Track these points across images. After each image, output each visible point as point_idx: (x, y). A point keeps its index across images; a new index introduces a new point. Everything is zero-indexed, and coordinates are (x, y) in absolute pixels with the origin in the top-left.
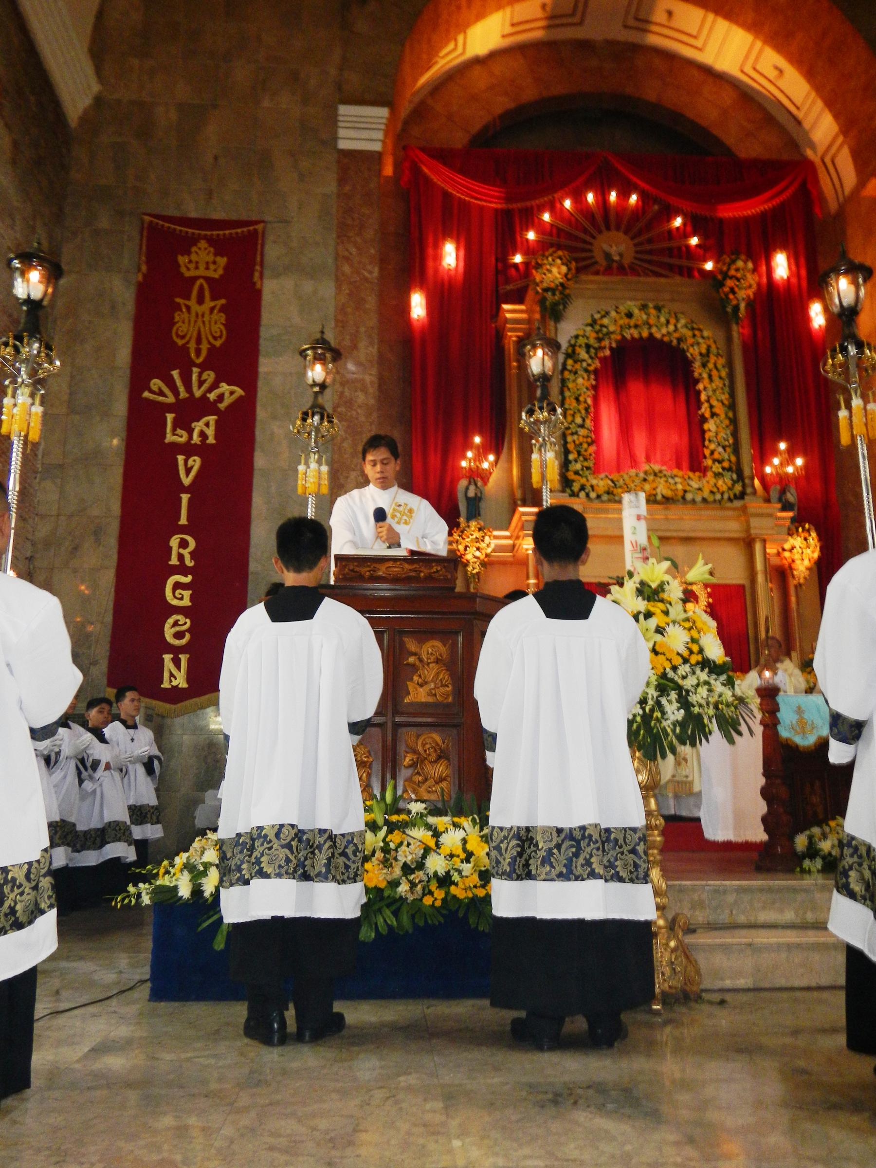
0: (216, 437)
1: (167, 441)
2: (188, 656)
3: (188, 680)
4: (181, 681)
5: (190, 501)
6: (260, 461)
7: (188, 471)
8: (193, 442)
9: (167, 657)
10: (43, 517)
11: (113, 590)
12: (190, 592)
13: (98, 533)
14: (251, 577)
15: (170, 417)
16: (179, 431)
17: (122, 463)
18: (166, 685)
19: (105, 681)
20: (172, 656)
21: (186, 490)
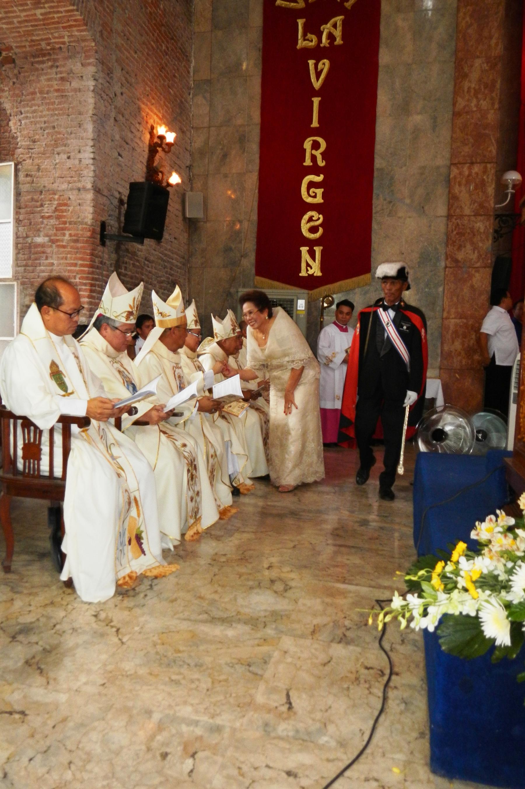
0: (343, 38)
1: (298, 47)
2: (321, 248)
3: (322, 269)
4: (316, 270)
5: (320, 103)
6: (385, 57)
7: (318, 74)
8: (322, 45)
9: (304, 250)
10: (197, 129)
11: (257, 191)
12: (322, 190)
13: (242, 140)
14: (376, 174)
15: (301, 22)
16: (309, 36)
17: (260, 73)
18: (303, 273)
19: (253, 271)
20: (307, 248)
21: (316, 93)
